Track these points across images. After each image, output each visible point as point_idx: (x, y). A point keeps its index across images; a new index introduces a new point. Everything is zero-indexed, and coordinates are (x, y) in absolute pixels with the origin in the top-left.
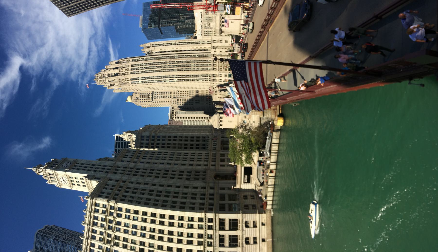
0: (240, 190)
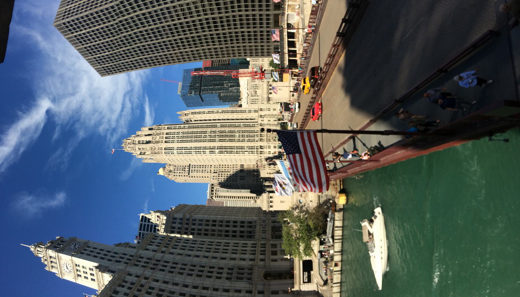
0: (299, 292)
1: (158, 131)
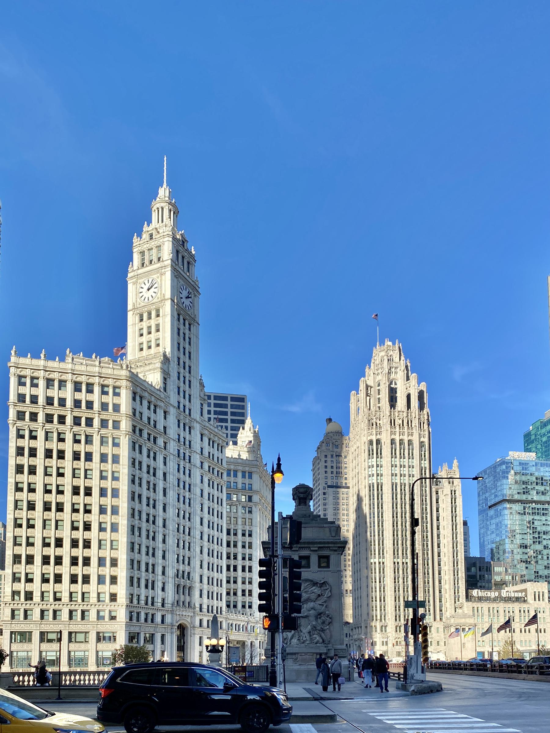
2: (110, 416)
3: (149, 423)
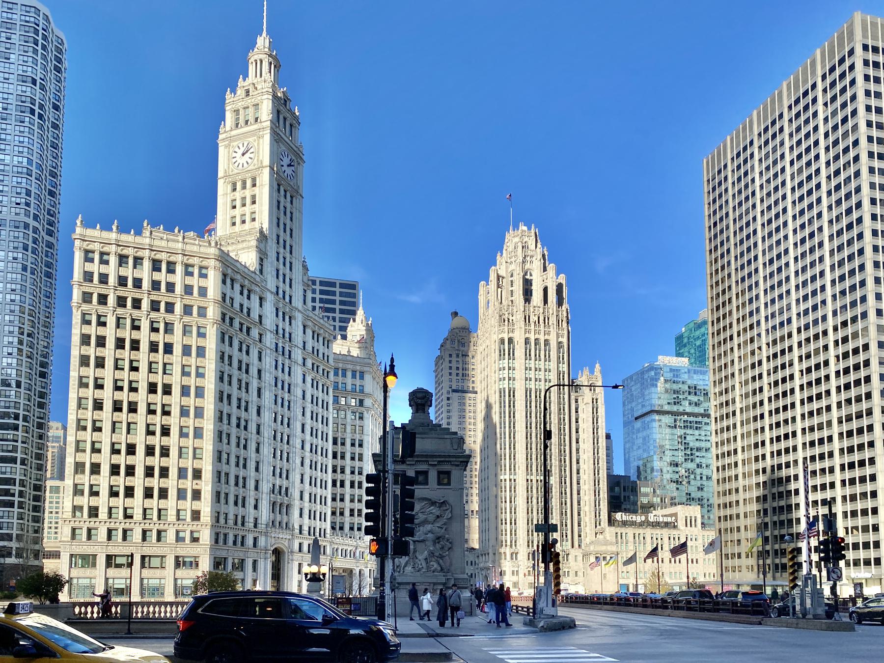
1: (553, 320)
2: (195, 301)
3: (242, 311)
